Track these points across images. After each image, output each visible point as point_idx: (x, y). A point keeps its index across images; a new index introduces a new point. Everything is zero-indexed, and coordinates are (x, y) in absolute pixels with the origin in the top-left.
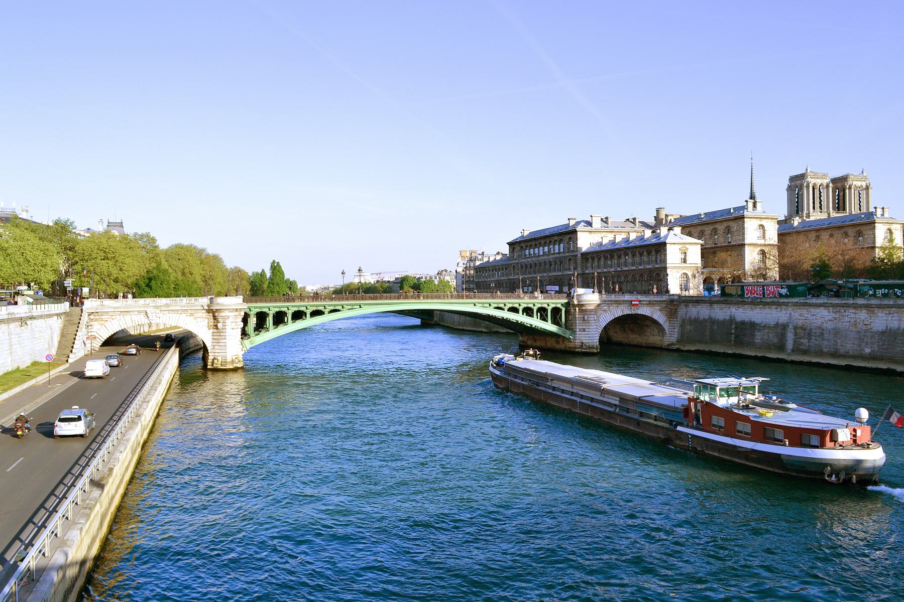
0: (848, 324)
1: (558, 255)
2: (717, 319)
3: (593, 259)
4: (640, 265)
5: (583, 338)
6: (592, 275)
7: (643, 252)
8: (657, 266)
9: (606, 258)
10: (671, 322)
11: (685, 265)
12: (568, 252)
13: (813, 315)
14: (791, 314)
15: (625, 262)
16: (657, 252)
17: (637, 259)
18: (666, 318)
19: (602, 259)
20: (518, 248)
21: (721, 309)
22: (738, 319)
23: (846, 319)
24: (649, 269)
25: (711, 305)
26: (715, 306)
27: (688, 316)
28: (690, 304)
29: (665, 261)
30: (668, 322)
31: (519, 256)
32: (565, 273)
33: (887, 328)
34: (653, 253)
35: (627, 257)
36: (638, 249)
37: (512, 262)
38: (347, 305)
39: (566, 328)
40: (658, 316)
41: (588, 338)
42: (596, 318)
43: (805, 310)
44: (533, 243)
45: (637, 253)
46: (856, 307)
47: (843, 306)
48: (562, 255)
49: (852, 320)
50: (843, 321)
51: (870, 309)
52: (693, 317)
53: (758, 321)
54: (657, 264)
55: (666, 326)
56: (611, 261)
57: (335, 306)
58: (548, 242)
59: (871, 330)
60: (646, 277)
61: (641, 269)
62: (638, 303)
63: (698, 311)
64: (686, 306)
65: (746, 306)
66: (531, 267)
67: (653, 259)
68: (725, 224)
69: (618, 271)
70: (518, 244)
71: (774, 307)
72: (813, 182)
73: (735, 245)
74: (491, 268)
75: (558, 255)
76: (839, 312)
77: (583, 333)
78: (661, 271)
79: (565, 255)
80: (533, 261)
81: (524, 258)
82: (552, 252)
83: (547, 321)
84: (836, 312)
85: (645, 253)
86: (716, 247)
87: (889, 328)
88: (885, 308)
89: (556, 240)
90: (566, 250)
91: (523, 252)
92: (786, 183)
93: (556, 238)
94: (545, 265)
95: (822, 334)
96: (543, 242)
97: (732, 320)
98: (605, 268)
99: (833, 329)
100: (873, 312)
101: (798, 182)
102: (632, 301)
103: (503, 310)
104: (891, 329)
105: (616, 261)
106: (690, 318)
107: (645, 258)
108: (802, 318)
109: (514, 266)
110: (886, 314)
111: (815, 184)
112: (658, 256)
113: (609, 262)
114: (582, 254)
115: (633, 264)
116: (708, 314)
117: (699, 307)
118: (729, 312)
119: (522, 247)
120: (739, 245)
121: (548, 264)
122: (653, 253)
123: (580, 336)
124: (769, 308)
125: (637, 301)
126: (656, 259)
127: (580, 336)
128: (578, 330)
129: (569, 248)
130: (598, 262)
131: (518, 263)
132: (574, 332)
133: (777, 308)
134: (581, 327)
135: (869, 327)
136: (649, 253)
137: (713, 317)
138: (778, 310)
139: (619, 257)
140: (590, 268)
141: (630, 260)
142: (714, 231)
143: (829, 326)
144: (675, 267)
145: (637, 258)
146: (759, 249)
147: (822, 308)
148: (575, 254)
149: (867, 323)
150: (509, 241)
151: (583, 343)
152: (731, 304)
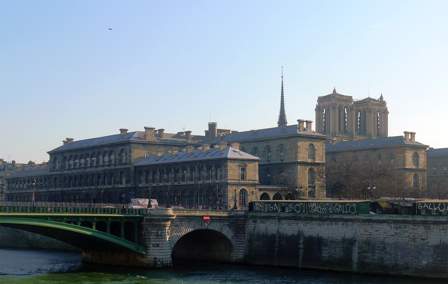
0: (408, 238)
1: (108, 168)
2: (285, 234)
3: (147, 173)
4: (199, 179)
5: (156, 254)
6: (146, 189)
7: (203, 167)
9: (162, 172)
10: (239, 238)
11: (243, 182)
12: (120, 164)
13: (376, 231)
14: (356, 230)
17: (196, 174)
19: (158, 173)
21: (290, 225)
23: (407, 235)
24: (209, 184)
25: (279, 221)
26: (283, 222)
27: (256, 231)
28: (258, 220)
29: (226, 176)
30: (235, 238)
31: (63, 167)
32: (116, 186)
33: (441, 241)
34: (213, 168)
35: (185, 172)
36: (197, 163)
39: (139, 244)
40: (228, 232)
41: (162, 254)
43: (369, 226)
44: (79, 154)
45: (196, 168)
46: (414, 223)
47: (404, 222)
48: (112, 167)
49: (411, 236)
50: (403, 236)
51: (427, 225)
54: (217, 179)
55: (234, 242)
56: (168, 175)
58: (96, 153)
59: (427, 244)
60: (205, 192)
62: (209, 218)
63: (266, 227)
64: (254, 222)
65: (314, 222)
66: (76, 179)
67: (213, 174)
68: (278, 142)
69: (175, 186)
71: (340, 223)
72: (339, 104)
73: (288, 163)
74: (26, 179)
75: (108, 168)
76: (400, 228)
77: (157, 248)
79: (117, 167)
80: (78, 173)
82: (101, 163)
84: (397, 228)
86: (269, 165)
87: (442, 242)
88: (439, 224)
89: (105, 152)
90: (117, 162)
91: (67, 162)
92: (315, 103)
95: (385, 248)
96: (90, 152)
97: (300, 234)
98: (161, 182)
99: (395, 243)
100: (429, 228)
101: (326, 103)
102: (203, 217)
103: (76, 224)
104: (444, 243)
105: (173, 175)
106: (258, 233)
107: (205, 174)
108: (366, 233)
109: (55, 178)
110: (440, 230)
111: (340, 105)
112: (218, 172)
113: (166, 177)
114: (135, 167)
115: (191, 179)
116: (276, 229)
117: (268, 223)
118: (297, 227)
119: (65, 157)
120: (292, 163)
121: (96, 176)
122: (213, 168)
123: (154, 251)
124: (336, 224)
126: (216, 174)
128: (151, 245)
129: (121, 160)
130: (153, 176)
131: (61, 174)
132: (146, 248)
133: (343, 224)
134: (155, 243)
135: (426, 241)
136: (209, 168)
137: (282, 232)
138: (344, 226)
139: (177, 171)
140: (144, 182)
141: (189, 175)
142: (267, 147)
143: (390, 241)
144: (234, 184)
146: (309, 168)
147: (384, 224)
148: (128, 166)
149: (424, 237)
150: (50, 150)
151: (156, 259)
152: (299, 220)
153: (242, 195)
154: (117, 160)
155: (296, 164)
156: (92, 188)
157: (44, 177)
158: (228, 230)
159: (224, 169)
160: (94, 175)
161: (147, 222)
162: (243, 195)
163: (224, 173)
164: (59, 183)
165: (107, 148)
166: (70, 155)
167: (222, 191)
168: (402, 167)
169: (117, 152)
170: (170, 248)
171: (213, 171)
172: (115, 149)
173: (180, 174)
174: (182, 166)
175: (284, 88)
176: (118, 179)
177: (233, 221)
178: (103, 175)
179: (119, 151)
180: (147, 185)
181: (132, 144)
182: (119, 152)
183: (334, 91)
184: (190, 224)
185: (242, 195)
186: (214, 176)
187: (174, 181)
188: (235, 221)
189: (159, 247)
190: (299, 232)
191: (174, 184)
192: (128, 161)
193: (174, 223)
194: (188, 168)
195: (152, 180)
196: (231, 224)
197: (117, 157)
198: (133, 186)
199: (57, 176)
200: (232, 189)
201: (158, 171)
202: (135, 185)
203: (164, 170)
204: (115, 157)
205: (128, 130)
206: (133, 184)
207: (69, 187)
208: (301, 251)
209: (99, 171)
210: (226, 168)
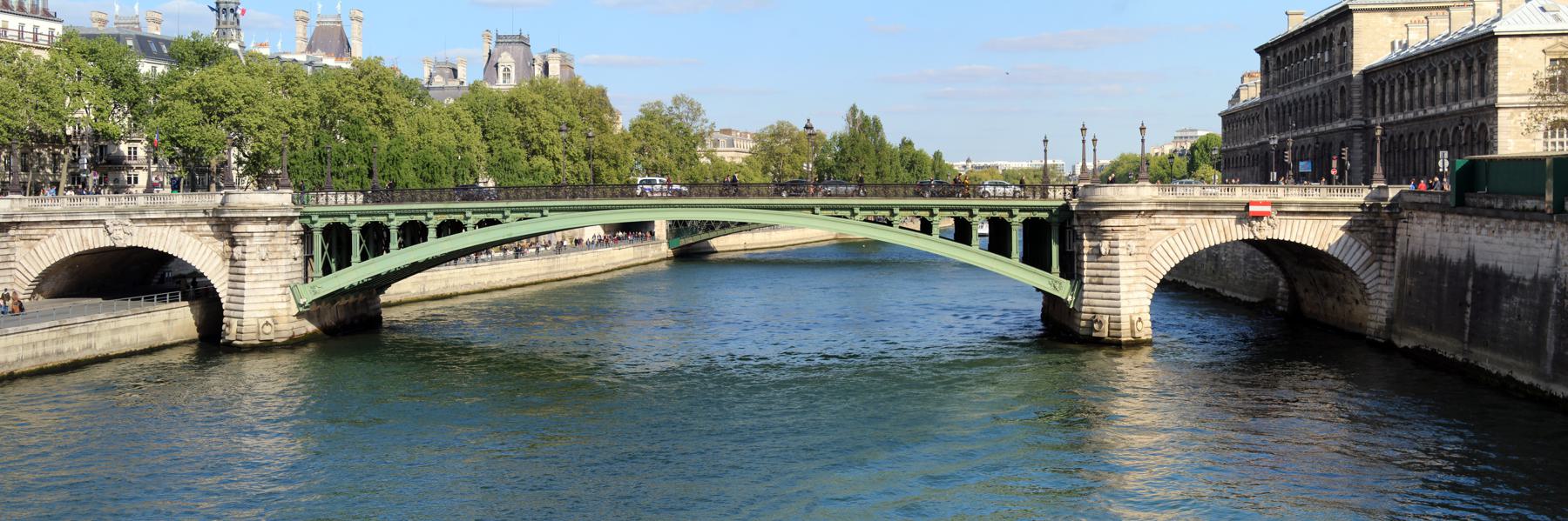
7: (1459, 63)
18: (1368, 254)
20: (1272, 62)
22: (1479, 262)
25: (1443, 219)
38: (515, 210)
42: (1134, 250)
52: (1416, 253)
53: (1507, 268)
57: (486, 211)
62: (1268, 209)
67: (1476, 83)
78: (1487, 116)
83: (1009, 256)
85: (1463, 66)
96: (1306, 42)
106: (1412, 254)
114: (1368, 74)
116: (1437, 242)
123: (1091, 294)
125: (1265, 203)
127: (1091, 294)
128: (1085, 280)
131: (1271, 102)
134: (1094, 272)
137: (1443, 252)
153: (1550, 140)
158: (1348, 244)
161: (1079, 218)
162: (1561, 140)
166: (1283, 53)
170: (1145, 287)
176: (1337, 108)
177: (1365, 218)
184: (1213, 224)
185: (1550, 140)
188: (1371, 218)
189: (1101, 284)
190: (1468, 255)
191: (1417, 113)
193: (1158, 221)
194: (1439, 70)
196: (1360, 226)
198: (1358, 123)
200: (1515, 123)
201: (1397, 81)
202: (1366, 121)
206: (1361, 120)
208: (1469, 310)
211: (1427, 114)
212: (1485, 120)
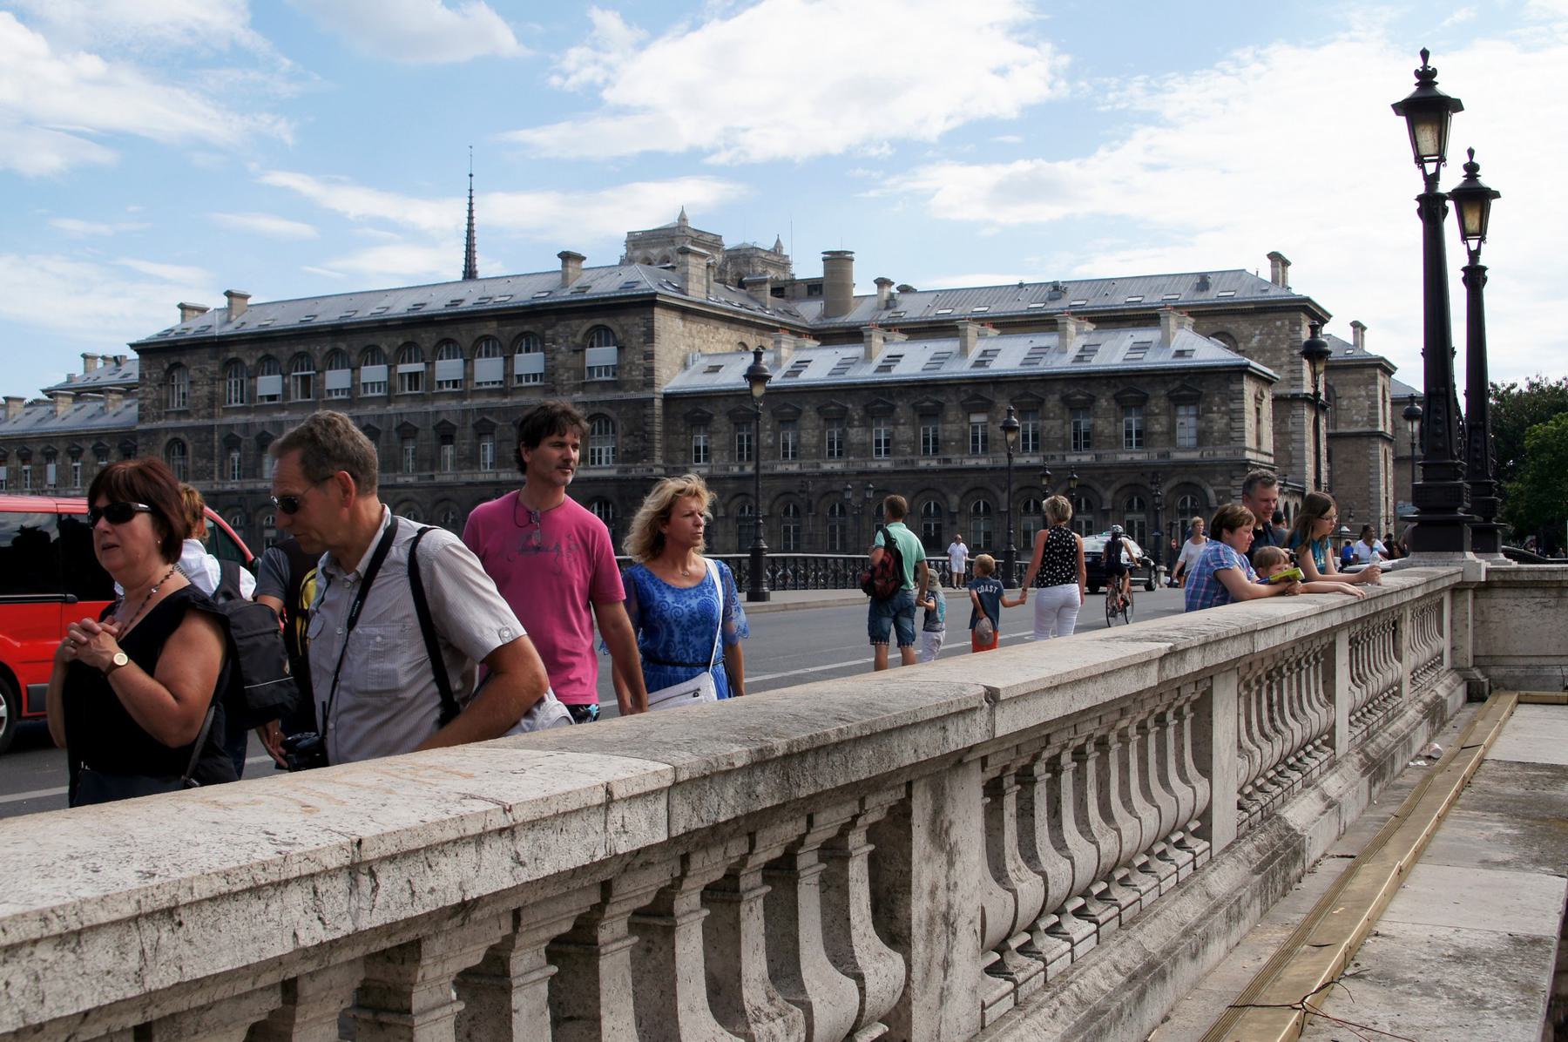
6: (731, 485)
8: (1178, 456)
15: (965, 434)
16: (1177, 400)
31: (212, 400)
34: (1158, 404)
36: (1058, 387)
37: (161, 424)
45: (1053, 401)
60: (1108, 495)
61: (1080, 468)
70: (206, 353)
81: (238, 410)
89: (486, 338)
93: (491, 328)
94: (403, 439)
109: (175, 441)
114: (669, 398)
131: (210, 429)
145: (1049, 424)
154: (561, 371)
155: (1298, 404)
156: (401, 480)
157: (94, 442)
159: (1223, 408)
160: (416, 430)
163: (1219, 423)
164: (194, 463)
165: (494, 324)
166: (261, 354)
167: (1211, 492)
168: (1368, 429)
169: (561, 341)
171: (1158, 414)
172: (552, 327)
173: (948, 427)
174: (963, 397)
175: (474, 207)
178: (469, 431)
179: (575, 336)
180: (742, 468)
181: (657, 310)
182: (579, 339)
183: (682, 218)
186: (1162, 433)
187: (913, 453)
192: (637, 375)
195: (772, 447)
197: (560, 357)
199: (182, 436)
203: (847, 409)
204: (553, 359)
205: (584, 258)
207: (255, 476)
209: (443, 416)
210: (1232, 406)
211: (949, 466)
212: (1196, 479)
